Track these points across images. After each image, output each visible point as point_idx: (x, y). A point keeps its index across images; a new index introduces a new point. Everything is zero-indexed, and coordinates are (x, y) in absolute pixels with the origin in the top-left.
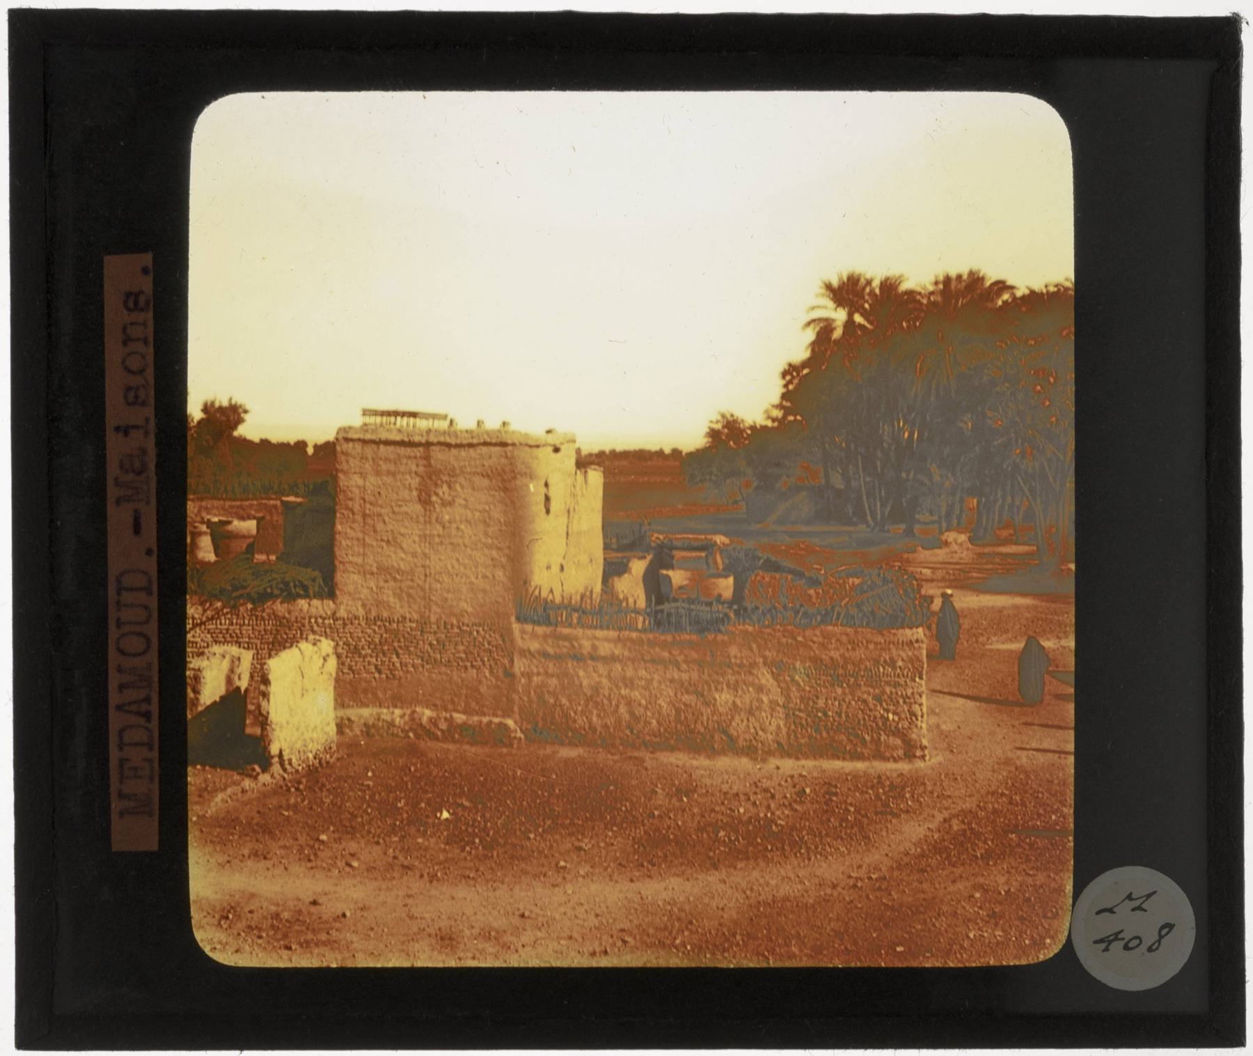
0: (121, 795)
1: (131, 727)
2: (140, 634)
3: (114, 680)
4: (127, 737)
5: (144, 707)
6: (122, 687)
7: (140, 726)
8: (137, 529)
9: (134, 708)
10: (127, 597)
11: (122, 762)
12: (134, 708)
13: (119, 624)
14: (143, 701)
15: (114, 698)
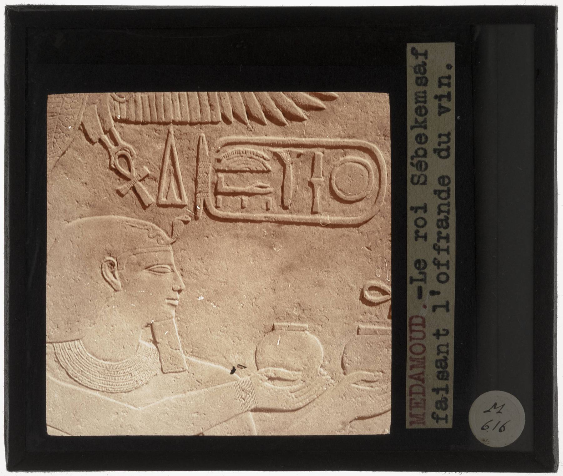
0: (411, 415)
1: (416, 385)
2: (420, 344)
3: (409, 363)
4: (415, 389)
5: (422, 376)
6: (412, 367)
7: (420, 385)
8: (420, 296)
9: (416, 376)
10: (414, 328)
11: (411, 400)
12: (416, 376)
13: (411, 339)
14: (421, 374)
15: (409, 372)
